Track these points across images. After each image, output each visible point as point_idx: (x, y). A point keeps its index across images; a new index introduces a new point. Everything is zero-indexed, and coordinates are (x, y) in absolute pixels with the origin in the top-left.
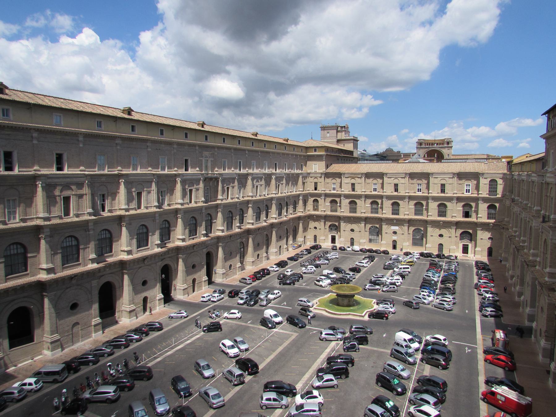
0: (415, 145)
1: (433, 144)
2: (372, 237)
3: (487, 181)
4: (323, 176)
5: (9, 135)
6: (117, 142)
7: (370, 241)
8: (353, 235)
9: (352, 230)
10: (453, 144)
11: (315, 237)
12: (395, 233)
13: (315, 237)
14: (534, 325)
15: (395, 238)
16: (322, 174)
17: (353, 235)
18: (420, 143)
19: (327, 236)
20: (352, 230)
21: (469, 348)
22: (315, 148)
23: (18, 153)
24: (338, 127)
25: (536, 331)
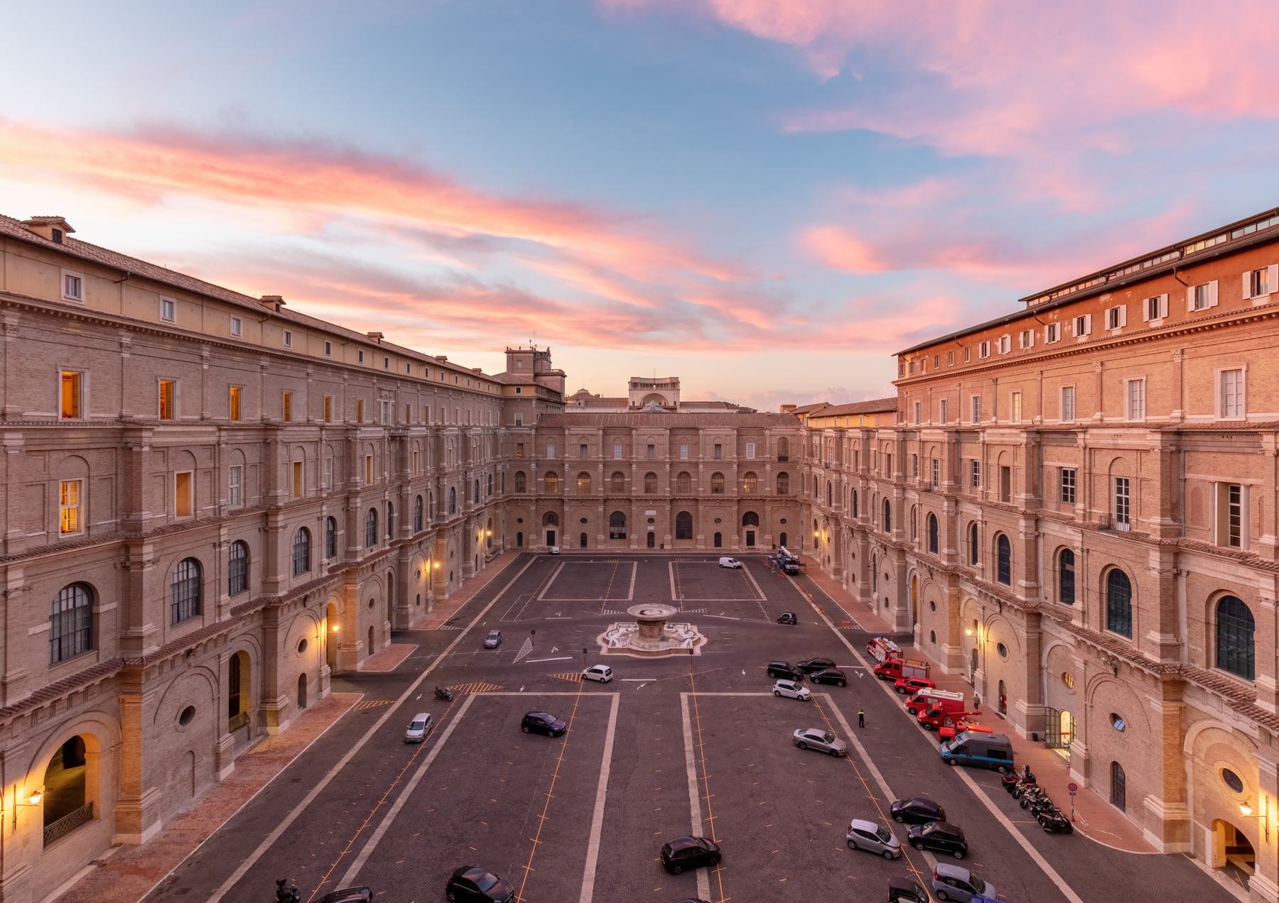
0: (627, 386)
1: (651, 385)
2: (615, 530)
3: (775, 440)
4: (533, 432)
5: (76, 335)
6: (263, 363)
7: (612, 536)
8: (586, 528)
9: (584, 521)
10: (681, 386)
11: (520, 536)
12: (651, 520)
13: (520, 536)
14: (917, 628)
15: (651, 528)
16: (531, 428)
17: (586, 528)
18: (635, 384)
19: (538, 533)
20: (584, 521)
21: (860, 671)
22: (518, 387)
23: (92, 378)
24: (535, 353)
25: (921, 635)
